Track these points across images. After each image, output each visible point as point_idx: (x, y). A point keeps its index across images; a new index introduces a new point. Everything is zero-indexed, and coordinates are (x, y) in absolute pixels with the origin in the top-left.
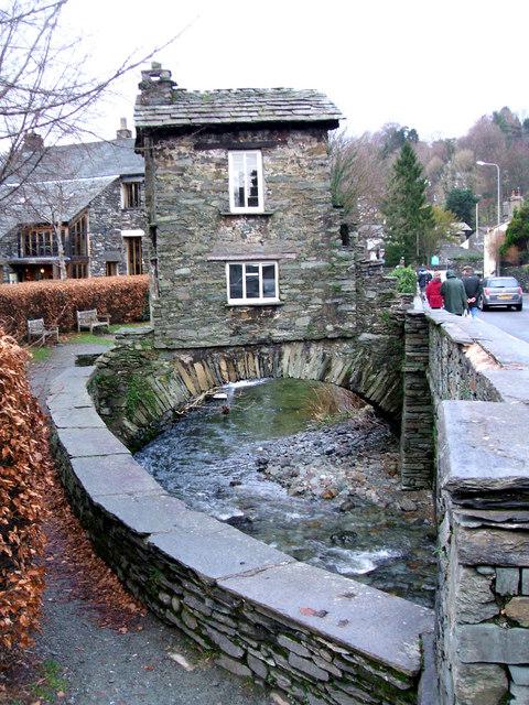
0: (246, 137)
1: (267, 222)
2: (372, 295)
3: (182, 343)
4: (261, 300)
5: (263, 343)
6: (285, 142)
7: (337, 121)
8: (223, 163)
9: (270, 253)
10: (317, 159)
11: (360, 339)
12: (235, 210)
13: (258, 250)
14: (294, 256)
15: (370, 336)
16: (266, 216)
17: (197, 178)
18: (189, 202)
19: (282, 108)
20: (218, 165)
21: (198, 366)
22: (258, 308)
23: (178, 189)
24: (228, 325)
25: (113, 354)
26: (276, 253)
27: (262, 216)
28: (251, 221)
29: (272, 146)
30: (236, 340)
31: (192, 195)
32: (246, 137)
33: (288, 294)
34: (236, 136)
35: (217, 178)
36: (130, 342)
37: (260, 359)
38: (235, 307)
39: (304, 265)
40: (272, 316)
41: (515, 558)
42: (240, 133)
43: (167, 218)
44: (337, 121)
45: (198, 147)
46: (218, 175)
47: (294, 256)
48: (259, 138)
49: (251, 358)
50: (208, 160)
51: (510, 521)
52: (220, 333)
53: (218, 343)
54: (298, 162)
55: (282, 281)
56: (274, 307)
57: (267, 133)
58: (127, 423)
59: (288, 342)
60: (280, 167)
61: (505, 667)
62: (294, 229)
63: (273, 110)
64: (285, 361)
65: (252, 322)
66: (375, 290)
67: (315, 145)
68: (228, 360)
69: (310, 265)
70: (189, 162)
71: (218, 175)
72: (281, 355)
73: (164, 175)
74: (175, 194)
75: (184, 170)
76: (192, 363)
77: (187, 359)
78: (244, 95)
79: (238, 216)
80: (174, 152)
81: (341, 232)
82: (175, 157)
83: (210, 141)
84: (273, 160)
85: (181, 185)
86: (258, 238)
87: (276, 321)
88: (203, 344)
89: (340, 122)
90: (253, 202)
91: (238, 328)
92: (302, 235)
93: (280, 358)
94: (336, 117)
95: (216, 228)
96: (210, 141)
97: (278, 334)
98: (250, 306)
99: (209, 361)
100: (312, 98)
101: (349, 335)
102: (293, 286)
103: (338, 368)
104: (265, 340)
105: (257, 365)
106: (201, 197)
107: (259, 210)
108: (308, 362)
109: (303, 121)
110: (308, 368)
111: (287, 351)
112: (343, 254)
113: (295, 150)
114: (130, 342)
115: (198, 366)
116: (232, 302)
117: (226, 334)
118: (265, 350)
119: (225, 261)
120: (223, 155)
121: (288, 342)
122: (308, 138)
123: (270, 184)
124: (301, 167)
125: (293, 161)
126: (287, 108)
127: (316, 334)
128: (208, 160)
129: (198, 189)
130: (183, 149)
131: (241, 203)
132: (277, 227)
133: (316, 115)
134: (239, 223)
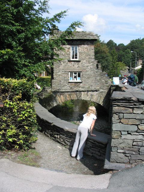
0: (75, 42)
2: (103, 81)
5: (77, 91)
8: (69, 49)
12: (72, 59)
15: (103, 91)
16: (79, 61)
20: (68, 49)
30: (71, 90)
39: (87, 73)
40: (80, 85)
41: (123, 112)
46: (68, 51)
48: (78, 42)
49: (74, 95)
50: (66, 48)
51: (122, 105)
53: (67, 91)
56: (80, 83)
57: (80, 41)
59: (83, 91)
61: (120, 131)
68: (69, 95)
69: (89, 73)
71: (68, 51)
72: (81, 94)
81: (96, 65)
84: (81, 48)
90: (76, 58)
97: (81, 89)
101: (98, 90)
107: (77, 60)
109: (88, 39)
110: (88, 97)
112: (97, 71)
118: (78, 93)
121: (83, 91)
127: (90, 90)
129: (63, 54)
131: (73, 58)
133: (92, 38)
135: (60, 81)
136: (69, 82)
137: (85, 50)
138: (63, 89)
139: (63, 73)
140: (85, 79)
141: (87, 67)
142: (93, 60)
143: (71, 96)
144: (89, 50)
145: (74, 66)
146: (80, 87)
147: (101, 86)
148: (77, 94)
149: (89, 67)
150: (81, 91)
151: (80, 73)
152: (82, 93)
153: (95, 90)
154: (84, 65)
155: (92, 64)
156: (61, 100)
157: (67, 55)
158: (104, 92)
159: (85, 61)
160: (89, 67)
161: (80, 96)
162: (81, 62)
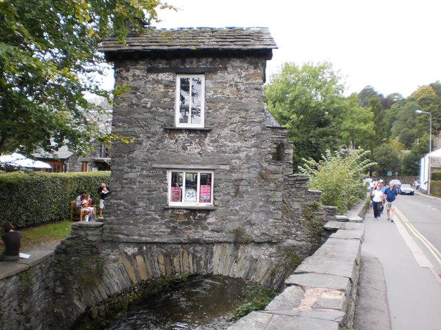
0: (191, 63)
1: (206, 137)
6: (226, 69)
8: (170, 85)
9: (207, 164)
10: (253, 84)
11: (285, 244)
12: (178, 125)
14: (227, 168)
16: (204, 132)
17: (148, 96)
18: (139, 116)
19: (227, 40)
20: (166, 86)
21: (139, 259)
22: (193, 211)
23: (132, 105)
24: (167, 225)
27: (202, 131)
28: (192, 135)
29: (214, 71)
30: (173, 238)
32: (191, 63)
34: (183, 62)
35: (165, 97)
36: (82, 233)
37: (194, 257)
38: (173, 209)
40: (205, 219)
42: (188, 60)
44: (271, 50)
45: (150, 71)
46: (165, 95)
47: (227, 168)
48: (204, 63)
49: (185, 255)
50: (158, 82)
52: (159, 230)
53: (157, 240)
54: (236, 86)
57: (210, 60)
58: (77, 303)
60: (220, 91)
62: (229, 144)
63: (217, 42)
64: (215, 259)
65: (188, 223)
67: (252, 71)
68: (166, 255)
70: (142, 83)
71: (165, 95)
72: (212, 254)
75: (137, 89)
76: (134, 255)
77: (130, 251)
78: (202, 31)
79: (180, 130)
80: (130, 74)
82: (131, 79)
83: (161, 66)
85: (134, 102)
86: (198, 150)
87: (209, 224)
88: (144, 239)
89: (274, 51)
91: (175, 228)
94: (269, 47)
95: (161, 140)
96: (161, 66)
97: (207, 235)
98: (186, 209)
99: (149, 256)
100: (258, 35)
101: (274, 241)
102: (228, 194)
103: (263, 268)
104: (197, 240)
105: (191, 262)
107: (201, 125)
108: (236, 262)
111: (217, 250)
112: (273, 167)
113: (235, 74)
114: (82, 233)
115: (139, 259)
116: (172, 204)
117: (164, 232)
118: (199, 248)
119: (168, 169)
120: (171, 78)
122: (246, 65)
123: (211, 104)
124: (238, 90)
125: (231, 85)
126: (230, 40)
128: (158, 82)
129: (149, 106)
130: (137, 72)
132: (215, 141)
134: (184, 136)
135: (134, 204)
137: (227, 92)
140: (226, 198)
141: (237, 152)
143: (171, 261)
144: (243, 93)
145: (185, 148)
149: (242, 155)
150: (213, 243)
153: (263, 238)
154: (224, 145)
155: (253, 141)
156: (136, 272)
157: (161, 110)
158: (301, 247)
159: (226, 131)
160: (242, 155)
161: (208, 262)
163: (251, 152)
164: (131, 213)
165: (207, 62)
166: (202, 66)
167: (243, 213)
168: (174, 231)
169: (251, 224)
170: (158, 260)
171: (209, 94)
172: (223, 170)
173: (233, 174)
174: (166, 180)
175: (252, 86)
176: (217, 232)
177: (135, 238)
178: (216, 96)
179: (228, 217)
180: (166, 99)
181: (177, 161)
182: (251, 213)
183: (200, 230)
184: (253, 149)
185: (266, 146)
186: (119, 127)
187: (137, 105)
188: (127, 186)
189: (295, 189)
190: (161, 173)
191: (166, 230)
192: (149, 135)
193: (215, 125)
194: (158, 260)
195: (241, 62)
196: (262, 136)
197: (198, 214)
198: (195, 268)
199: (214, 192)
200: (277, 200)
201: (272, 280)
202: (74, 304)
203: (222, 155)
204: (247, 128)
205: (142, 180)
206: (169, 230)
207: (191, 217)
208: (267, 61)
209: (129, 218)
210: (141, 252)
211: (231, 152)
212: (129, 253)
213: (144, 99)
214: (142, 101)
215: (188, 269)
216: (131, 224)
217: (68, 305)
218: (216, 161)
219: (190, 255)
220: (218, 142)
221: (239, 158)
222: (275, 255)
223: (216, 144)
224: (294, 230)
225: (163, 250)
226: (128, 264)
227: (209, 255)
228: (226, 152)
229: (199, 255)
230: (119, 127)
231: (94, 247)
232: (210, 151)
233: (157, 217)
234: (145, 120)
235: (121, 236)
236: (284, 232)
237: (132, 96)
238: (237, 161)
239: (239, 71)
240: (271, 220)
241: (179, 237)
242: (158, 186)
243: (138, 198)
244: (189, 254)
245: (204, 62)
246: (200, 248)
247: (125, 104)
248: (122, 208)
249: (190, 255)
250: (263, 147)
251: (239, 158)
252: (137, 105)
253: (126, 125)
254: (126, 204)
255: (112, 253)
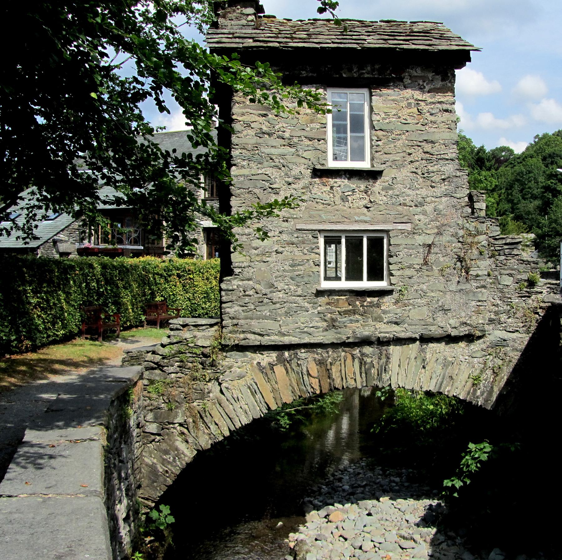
3: (259, 338)
4: (365, 284)
6: (401, 80)
7: (468, 51)
9: (378, 223)
13: (363, 218)
14: (408, 227)
18: (273, 151)
25: (166, 351)
26: (384, 222)
31: (281, 141)
32: (350, 70)
33: (402, 276)
35: (312, 122)
43: (246, 172)
44: (468, 51)
55: (391, 260)
59: (399, 341)
60: (394, 112)
62: (410, 192)
65: (354, 312)
66: (510, 275)
68: (321, 363)
73: (243, 114)
74: (255, 140)
85: (265, 129)
87: (385, 312)
88: (287, 340)
92: (420, 200)
93: (387, 363)
99: (294, 366)
101: (478, 333)
106: (290, 145)
107: (365, 165)
108: (424, 367)
110: (424, 375)
115: (279, 370)
117: (317, 328)
118: (368, 350)
119: (320, 231)
121: (399, 341)
122: (430, 75)
125: (410, 104)
127: (435, 331)
129: (287, 135)
136: (320, 293)
138: (284, 329)
139: (285, 237)
140: (408, 272)
141: (421, 205)
142: (450, 169)
145: (344, 199)
146: (379, 319)
147: (496, 313)
148: (363, 354)
149: (429, 208)
151: (382, 239)
152: (394, 350)
153: (463, 331)
155: (443, 188)
156: (274, 390)
158: (514, 340)
160: (429, 208)
162: (386, 178)
163: (441, 203)
164: (266, 301)
165: (373, 70)
166: (366, 76)
167: (433, 294)
168: (333, 325)
169: (446, 311)
170: (308, 371)
171: (378, 118)
172: (402, 231)
173: (416, 237)
174: (318, 248)
175: (439, 106)
176: (397, 323)
177: (272, 338)
178: (387, 121)
179: (411, 301)
180: (313, 125)
181: (334, 219)
182: (445, 293)
183: (370, 321)
184: (444, 199)
185: (462, 195)
186: (243, 167)
187: (270, 135)
188: (258, 258)
189: (504, 257)
190: (310, 237)
191: (319, 324)
192: (290, 180)
193: (388, 164)
194: (308, 371)
195: (422, 70)
196: (455, 180)
197: (369, 299)
198: (364, 379)
199: (389, 264)
200: (480, 273)
201: (475, 391)
202: (177, 449)
203: (400, 208)
204: (435, 168)
205: (281, 250)
206: (325, 324)
207: (358, 303)
208: (457, 72)
209: (264, 308)
210: (281, 361)
211: (413, 204)
212: (263, 364)
213: (280, 125)
214: (277, 127)
215: (353, 382)
216: (265, 318)
217: (166, 452)
218: (391, 218)
219: (356, 361)
220: (393, 189)
221: (424, 213)
222: (478, 355)
223: (390, 192)
224: (503, 317)
225: (316, 356)
226: (260, 379)
227: (384, 360)
228: (405, 205)
229: (369, 360)
230: (243, 167)
231: (205, 355)
232: (381, 203)
233: (306, 304)
234: (283, 156)
235: (251, 336)
236: (491, 321)
237: (261, 119)
238: (422, 217)
239: (421, 83)
240: (474, 303)
241: (339, 333)
242: (307, 257)
243: (276, 277)
244: (353, 359)
245: (369, 68)
246: (371, 349)
247: (251, 132)
248: (251, 292)
249: (356, 361)
250: (458, 196)
251: (424, 213)
252: (270, 135)
253: (252, 164)
254: (258, 287)
255: (236, 365)
